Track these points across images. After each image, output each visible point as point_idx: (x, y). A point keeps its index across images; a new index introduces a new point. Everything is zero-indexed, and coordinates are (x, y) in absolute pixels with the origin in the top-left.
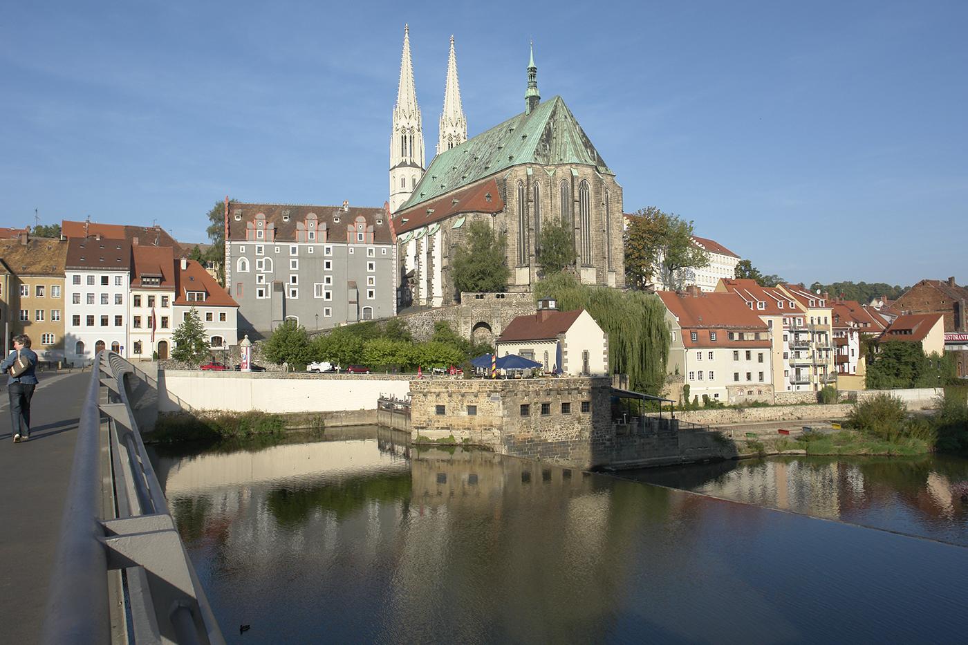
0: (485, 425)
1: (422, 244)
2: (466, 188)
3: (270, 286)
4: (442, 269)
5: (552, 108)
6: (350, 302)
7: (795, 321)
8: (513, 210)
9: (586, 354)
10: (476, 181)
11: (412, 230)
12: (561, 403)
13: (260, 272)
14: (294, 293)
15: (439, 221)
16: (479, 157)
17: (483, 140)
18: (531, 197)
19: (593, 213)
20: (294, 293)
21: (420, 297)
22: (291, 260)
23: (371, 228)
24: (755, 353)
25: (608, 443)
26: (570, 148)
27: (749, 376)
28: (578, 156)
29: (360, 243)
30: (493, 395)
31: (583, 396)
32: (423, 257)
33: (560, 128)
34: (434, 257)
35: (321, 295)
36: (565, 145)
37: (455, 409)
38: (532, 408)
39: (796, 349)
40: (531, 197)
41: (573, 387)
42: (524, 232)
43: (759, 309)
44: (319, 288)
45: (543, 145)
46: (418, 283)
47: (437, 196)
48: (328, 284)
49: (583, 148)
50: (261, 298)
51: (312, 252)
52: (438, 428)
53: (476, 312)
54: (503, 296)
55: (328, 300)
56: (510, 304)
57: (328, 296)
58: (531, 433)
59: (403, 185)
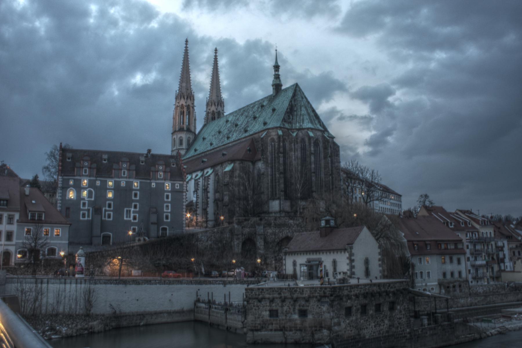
0: (316, 327)
1: (199, 183)
6: (152, 223)
7: (472, 235)
8: (267, 159)
9: (367, 262)
10: (239, 140)
11: (191, 173)
12: (374, 304)
17: (240, 114)
18: (281, 149)
19: (323, 162)
20: (109, 216)
24: (455, 258)
25: (408, 336)
26: (306, 117)
27: (452, 274)
28: (312, 123)
29: (158, 179)
30: (323, 300)
31: (390, 297)
32: (200, 192)
33: (299, 104)
34: (209, 192)
35: (130, 217)
36: (303, 115)
37: (287, 313)
38: (354, 309)
39: (476, 254)
41: (383, 290)
42: (275, 174)
43: (450, 227)
44: (129, 212)
46: (196, 211)
47: (208, 151)
48: (135, 210)
49: (315, 118)
52: (271, 330)
53: (247, 230)
55: (135, 221)
57: (135, 218)
58: (353, 332)
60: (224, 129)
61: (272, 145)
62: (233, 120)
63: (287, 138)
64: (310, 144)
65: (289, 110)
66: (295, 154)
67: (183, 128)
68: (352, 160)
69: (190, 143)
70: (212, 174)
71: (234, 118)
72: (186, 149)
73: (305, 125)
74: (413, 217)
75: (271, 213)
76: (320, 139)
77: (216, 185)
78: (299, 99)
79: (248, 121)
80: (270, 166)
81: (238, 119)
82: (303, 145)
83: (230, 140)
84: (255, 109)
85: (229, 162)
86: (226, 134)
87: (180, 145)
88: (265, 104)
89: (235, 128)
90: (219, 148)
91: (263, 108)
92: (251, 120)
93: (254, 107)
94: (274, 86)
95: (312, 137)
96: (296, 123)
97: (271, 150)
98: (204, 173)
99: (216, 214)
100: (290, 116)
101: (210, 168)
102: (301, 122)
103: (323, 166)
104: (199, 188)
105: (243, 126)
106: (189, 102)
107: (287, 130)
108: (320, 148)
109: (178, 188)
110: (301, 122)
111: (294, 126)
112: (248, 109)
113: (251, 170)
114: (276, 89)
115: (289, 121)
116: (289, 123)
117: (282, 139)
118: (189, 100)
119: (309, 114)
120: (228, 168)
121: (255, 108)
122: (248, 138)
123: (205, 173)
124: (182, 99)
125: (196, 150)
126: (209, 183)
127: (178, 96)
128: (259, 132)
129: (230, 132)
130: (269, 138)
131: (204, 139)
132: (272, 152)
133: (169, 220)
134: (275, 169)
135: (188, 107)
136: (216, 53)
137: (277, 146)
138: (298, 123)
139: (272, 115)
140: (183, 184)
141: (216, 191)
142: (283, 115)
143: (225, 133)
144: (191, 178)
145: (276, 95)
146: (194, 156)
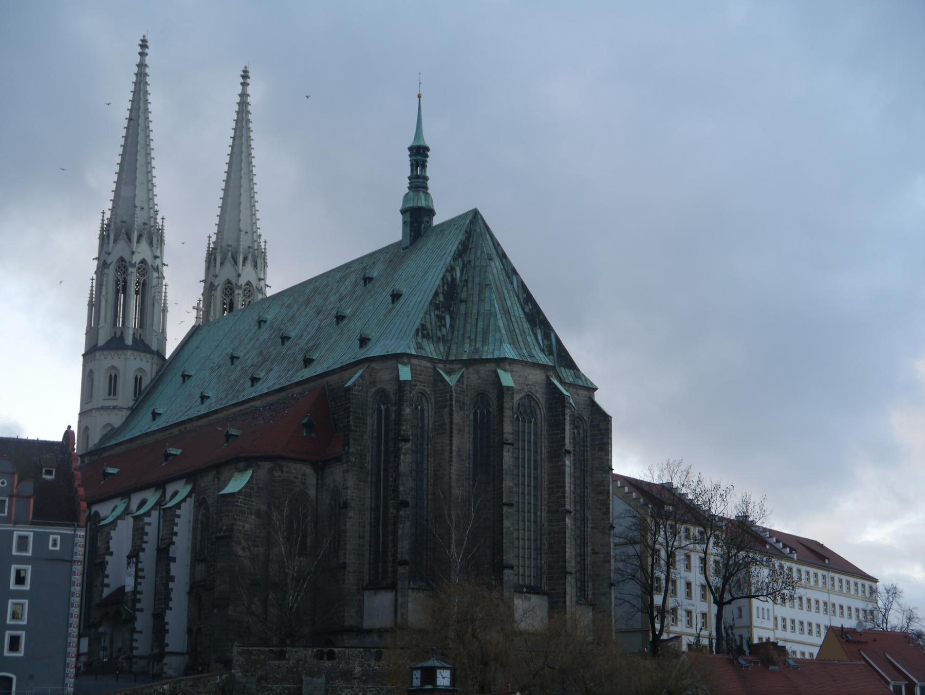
1: (147, 529)
2: (258, 403)
4: (192, 587)
5: (461, 237)
10: (282, 389)
11: (126, 494)
16: (292, 335)
21: (135, 653)
23: (28, 487)
28: (514, 343)
32: (148, 557)
33: (477, 280)
45: (437, 316)
46: (133, 619)
47: (191, 420)
49: (526, 326)
54: (331, 656)
56: (347, 675)
59: (113, 389)
61: (380, 410)
63: (427, 389)
65: (441, 298)
67: (122, 338)
68: (671, 461)
69: (143, 387)
70: (188, 500)
72: (128, 409)
73: (491, 347)
74: (785, 663)
75: (369, 632)
77: (199, 537)
78: (478, 263)
79: (319, 328)
81: (293, 316)
82: (482, 413)
83: (259, 388)
84: (346, 288)
85: (241, 465)
86: (252, 365)
87: (110, 394)
88: (375, 273)
89: (280, 347)
90: (225, 413)
91: (369, 286)
93: (342, 280)
94: (408, 214)
95: (509, 388)
96: (463, 342)
97: (375, 427)
98: (164, 494)
100: (444, 318)
101: (183, 482)
102: (479, 338)
103: (545, 485)
104: (144, 545)
106: (142, 251)
107: (429, 365)
108: (539, 425)
109: (58, 548)
110: (479, 338)
111: (454, 347)
112: (327, 286)
113: (312, 492)
114: (411, 222)
115: (439, 334)
116: (439, 339)
118: (144, 245)
120: (236, 484)
121: (347, 282)
122: (312, 385)
123: (169, 494)
124: (122, 243)
125: (155, 415)
126: (176, 529)
127: (107, 230)
128: (343, 369)
129: (264, 361)
131: (185, 377)
133: (21, 654)
135: (143, 267)
136: (245, 85)
137: (393, 415)
138: (467, 341)
139: (390, 311)
140: (74, 536)
141: (198, 557)
142: (422, 315)
143: (249, 362)
144: (126, 512)
145: (412, 244)
146: (147, 434)
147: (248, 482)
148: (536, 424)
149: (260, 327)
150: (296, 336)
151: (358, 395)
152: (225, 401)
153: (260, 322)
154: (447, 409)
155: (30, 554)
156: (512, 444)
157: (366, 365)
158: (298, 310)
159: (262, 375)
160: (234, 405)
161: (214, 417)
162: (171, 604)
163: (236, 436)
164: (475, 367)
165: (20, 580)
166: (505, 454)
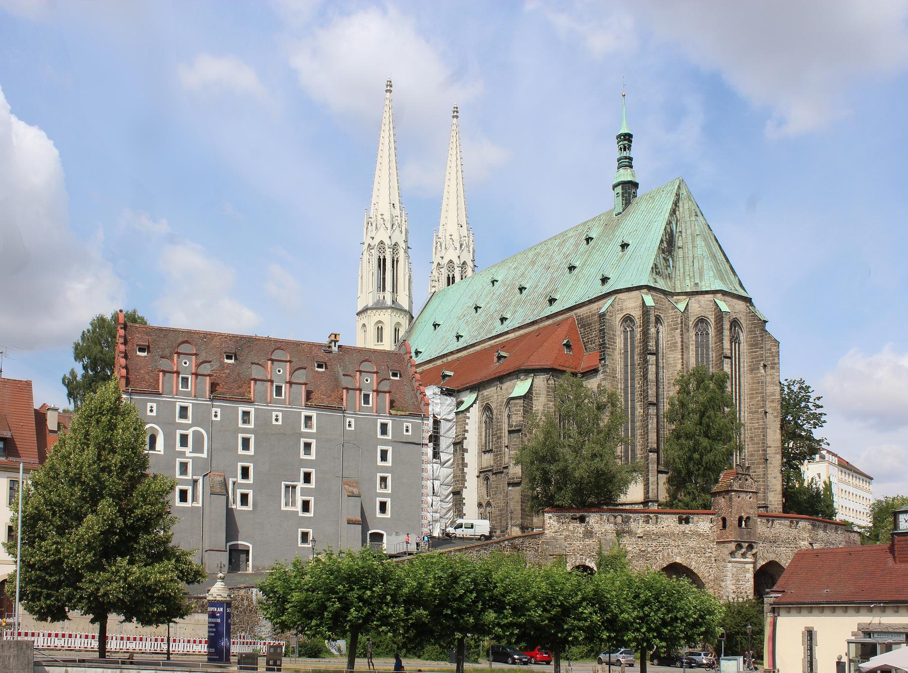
2: (512, 336)
3: (200, 481)
4: (481, 472)
8: (614, 370)
10: (533, 323)
13: (183, 454)
14: (244, 498)
15: (475, 388)
20: (244, 498)
22: (240, 436)
34: (466, 451)
35: (294, 504)
40: (652, 343)
48: (307, 486)
50: (183, 504)
51: (280, 423)
55: (307, 515)
57: (306, 506)
60: (488, 299)
62: (510, 278)
63: (662, 316)
64: (720, 331)
66: (683, 358)
70: (474, 405)
71: (512, 272)
76: (743, 322)
77: (484, 434)
80: (619, 386)
81: (523, 275)
84: (568, 249)
89: (519, 295)
92: (563, 274)
97: (622, 346)
99: (484, 505)
105: (540, 290)
108: (742, 345)
109: (410, 433)
112: (548, 250)
117: (653, 319)
119: (714, 257)
121: (568, 244)
128: (591, 302)
129: (507, 306)
130: (620, 316)
132: (626, 351)
134: (633, 393)
137: (639, 335)
143: (492, 309)
147: (530, 389)
148: (739, 344)
149: (493, 286)
150: (531, 287)
151: (610, 320)
152: (480, 337)
153: (493, 282)
154: (679, 331)
155: (390, 438)
156: (730, 358)
157: (613, 297)
158: (526, 269)
159: (508, 316)
160: (490, 339)
161: (472, 349)
162: (466, 484)
163: (505, 357)
164: (697, 298)
165: (384, 457)
166: (724, 365)
